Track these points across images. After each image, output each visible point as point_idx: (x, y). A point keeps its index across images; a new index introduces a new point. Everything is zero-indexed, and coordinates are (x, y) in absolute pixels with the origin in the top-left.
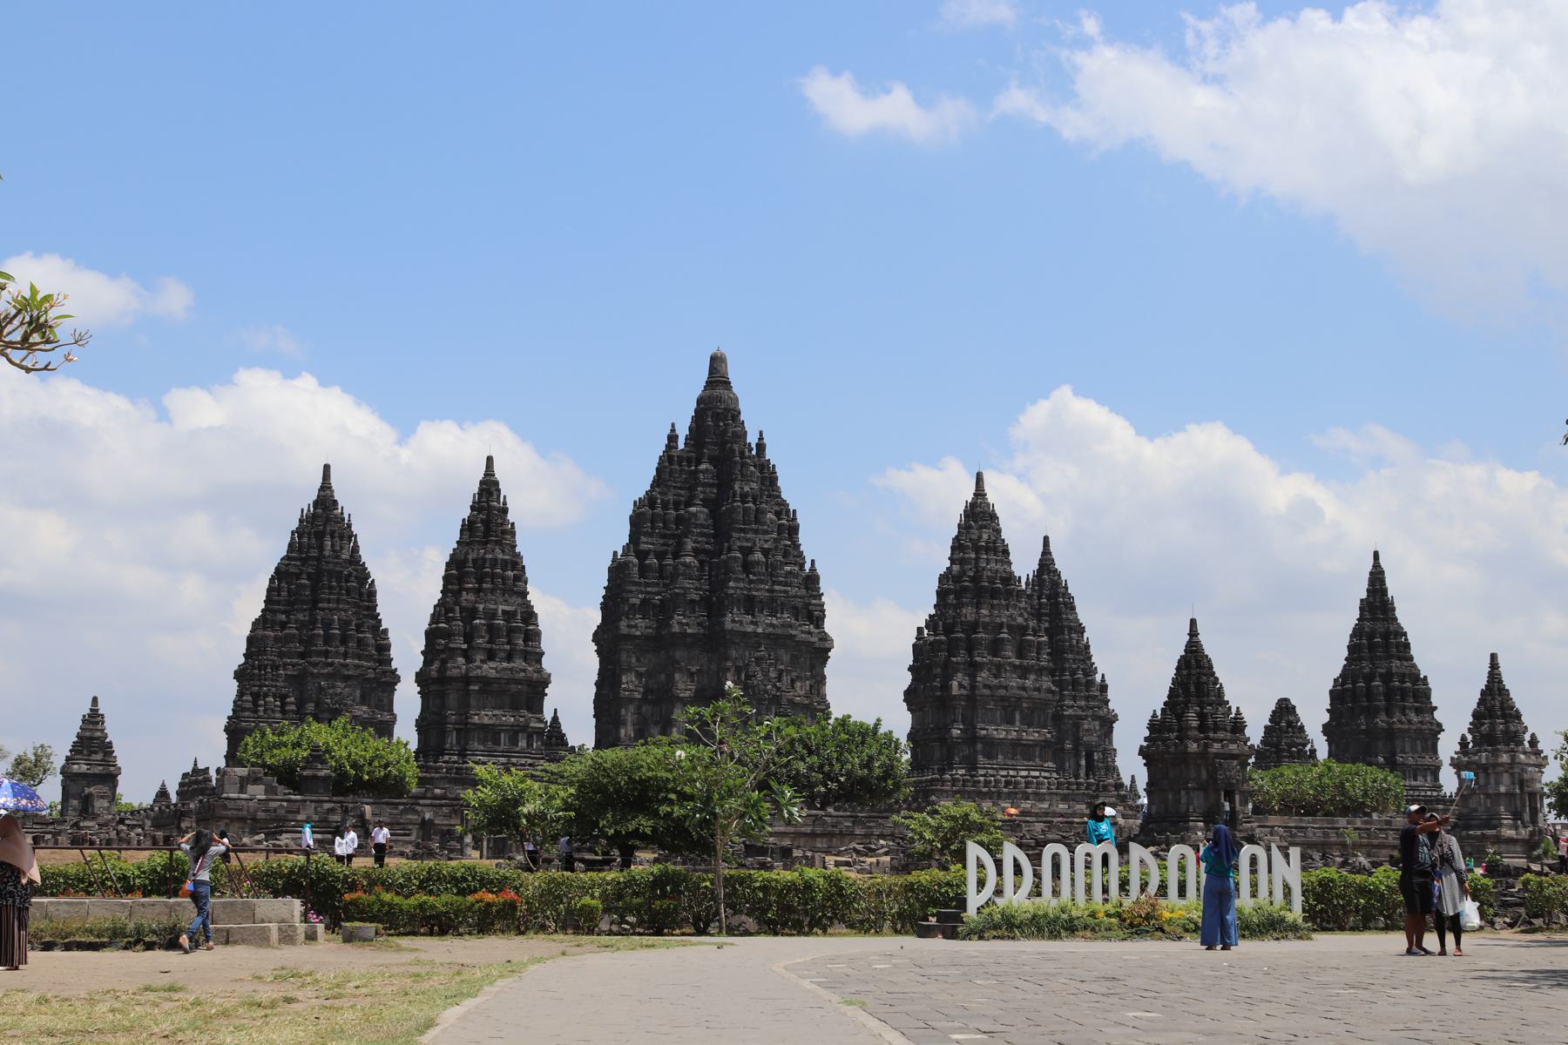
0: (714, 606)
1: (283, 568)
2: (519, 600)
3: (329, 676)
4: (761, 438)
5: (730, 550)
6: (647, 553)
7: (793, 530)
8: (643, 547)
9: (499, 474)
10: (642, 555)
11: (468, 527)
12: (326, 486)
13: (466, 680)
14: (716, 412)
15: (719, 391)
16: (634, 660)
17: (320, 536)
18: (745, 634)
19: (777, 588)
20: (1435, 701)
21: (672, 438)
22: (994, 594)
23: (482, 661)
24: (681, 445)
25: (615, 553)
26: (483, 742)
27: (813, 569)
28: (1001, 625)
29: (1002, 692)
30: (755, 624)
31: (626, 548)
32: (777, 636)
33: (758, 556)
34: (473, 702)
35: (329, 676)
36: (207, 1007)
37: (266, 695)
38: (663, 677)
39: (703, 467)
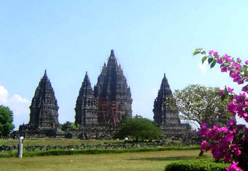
3: (48, 108)
4: (120, 65)
7: (126, 81)
9: (88, 74)
10: (100, 85)
11: (83, 83)
12: (45, 74)
14: (112, 60)
18: (119, 99)
19: (125, 91)
21: (105, 65)
24: (106, 66)
25: (95, 85)
26: (88, 120)
31: (97, 84)
35: (48, 108)
36: (77, 166)
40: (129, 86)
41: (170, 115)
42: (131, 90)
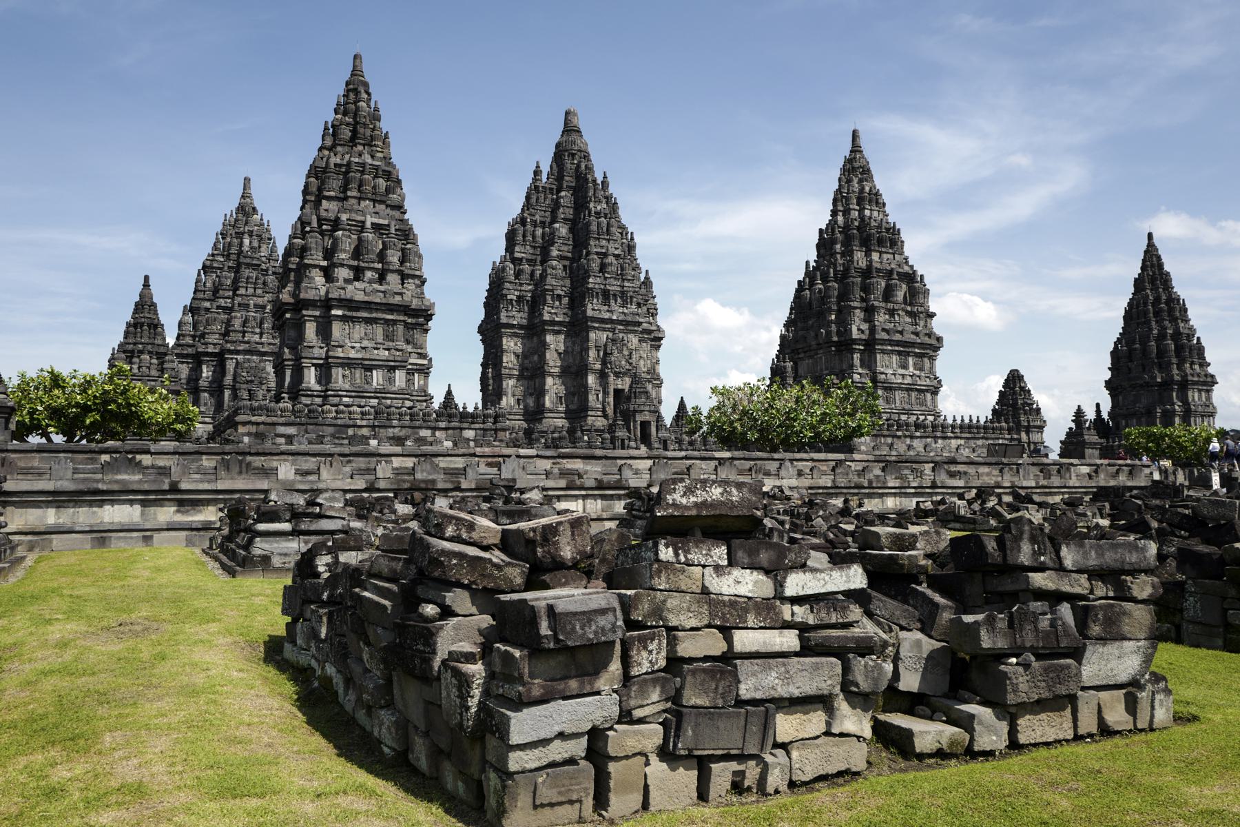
0: (577, 297)
1: (208, 263)
2: (397, 214)
4: (605, 177)
5: (588, 254)
6: (521, 259)
8: (517, 255)
10: (515, 261)
13: (326, 304)
15: (574, 136)
16: (512, 344)
17: (240, 235)
18: (603, 321)
19: (626, 284)
21: (537, 173)
22: (881, 242)
24: (544, 180)
25: (494, 263)
27: (647, 278)
28: (891, 272)
29: (898, 337)
30: (611, 312)
32: (627, 323)
33: (611, 259)
34: (337, 329)
37: (141, 352)
38: (536, 358)
39: (563, 194)
41: (901, 371)
42: (656, 290)
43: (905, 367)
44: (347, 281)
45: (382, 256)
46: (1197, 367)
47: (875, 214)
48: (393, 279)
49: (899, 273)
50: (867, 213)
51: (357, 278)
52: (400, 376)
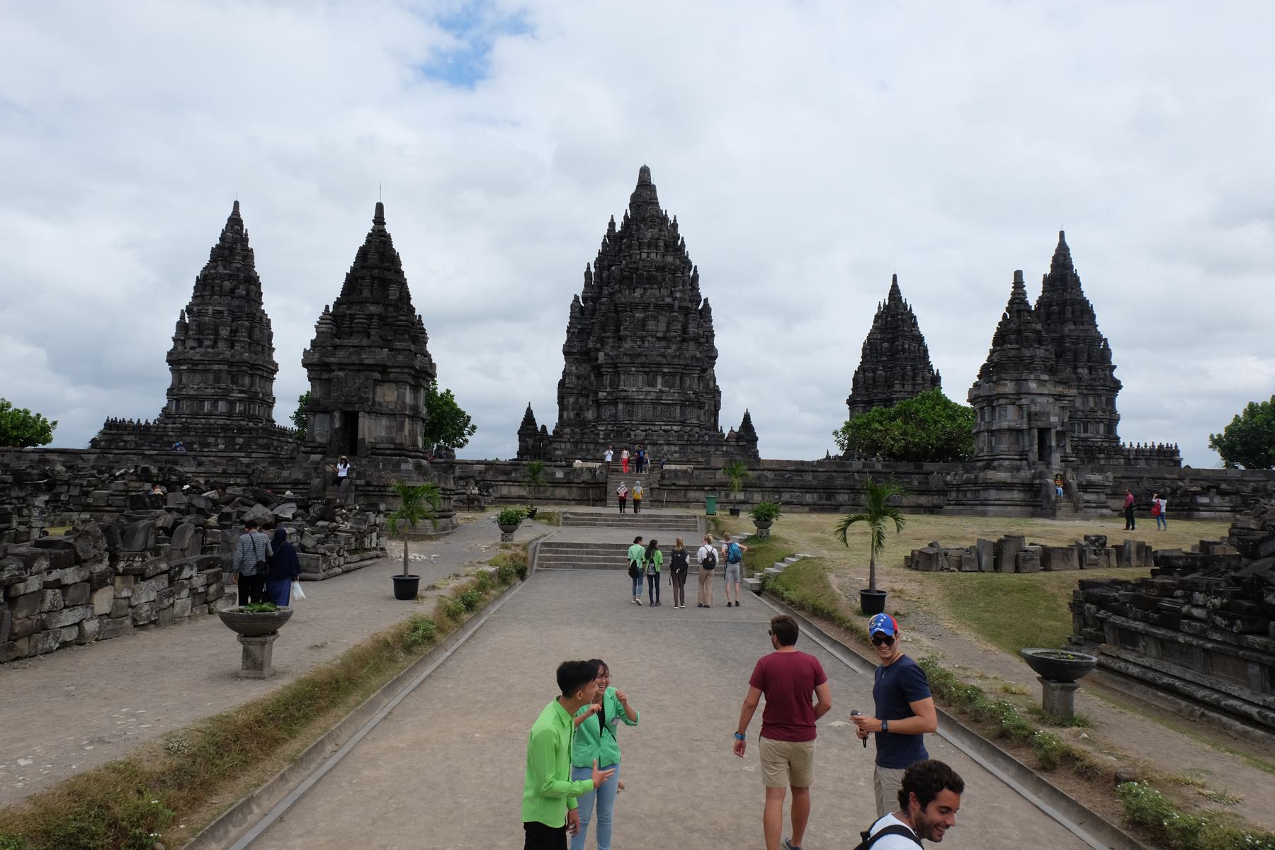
20: (1114, 361)
21: (612, 224)
23: (192, 348)
24: (618, 228)
29: (643, 359)
34: (184, 380)
40: (706, 300)
41: (646, 389)
42: (714, 314)
43: (654, 385)
44: (192, 348)
45: (217, 333)
46: (1084, 372)
47: (653, 256)
48: (221, 345)
49: (656, 306)
50: (644, 256)
51: (200, 345)
52: (222, 406)
